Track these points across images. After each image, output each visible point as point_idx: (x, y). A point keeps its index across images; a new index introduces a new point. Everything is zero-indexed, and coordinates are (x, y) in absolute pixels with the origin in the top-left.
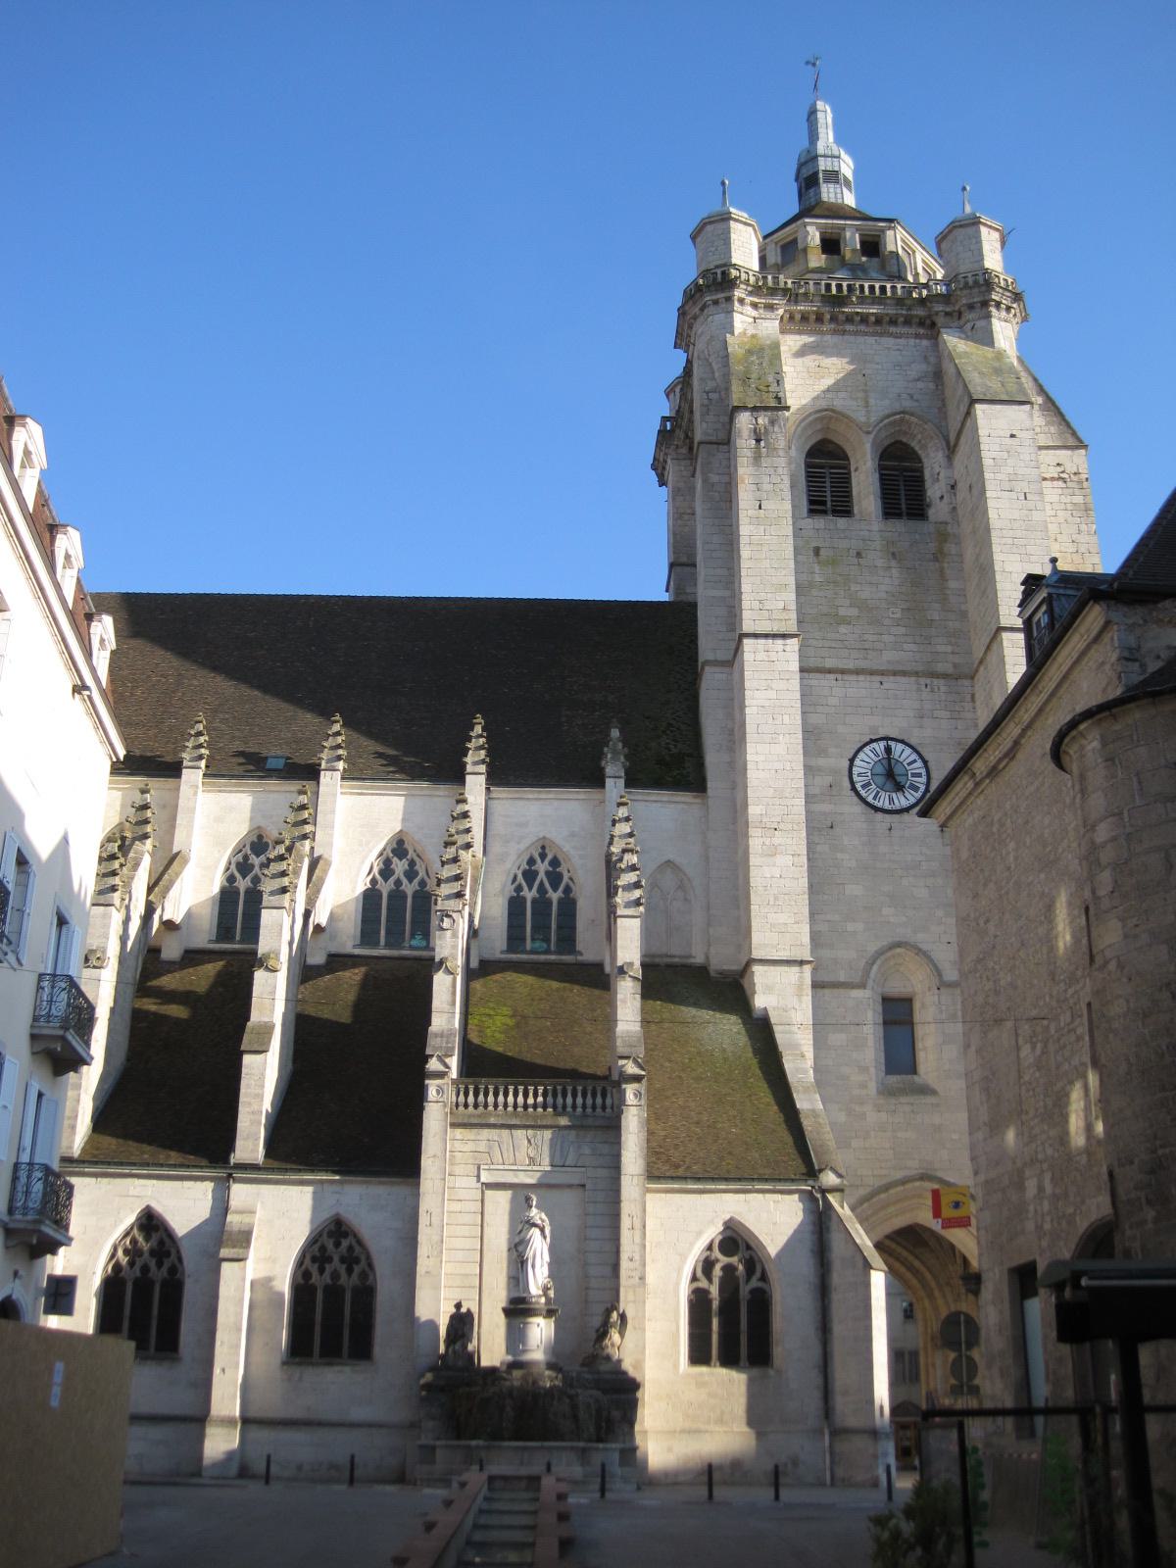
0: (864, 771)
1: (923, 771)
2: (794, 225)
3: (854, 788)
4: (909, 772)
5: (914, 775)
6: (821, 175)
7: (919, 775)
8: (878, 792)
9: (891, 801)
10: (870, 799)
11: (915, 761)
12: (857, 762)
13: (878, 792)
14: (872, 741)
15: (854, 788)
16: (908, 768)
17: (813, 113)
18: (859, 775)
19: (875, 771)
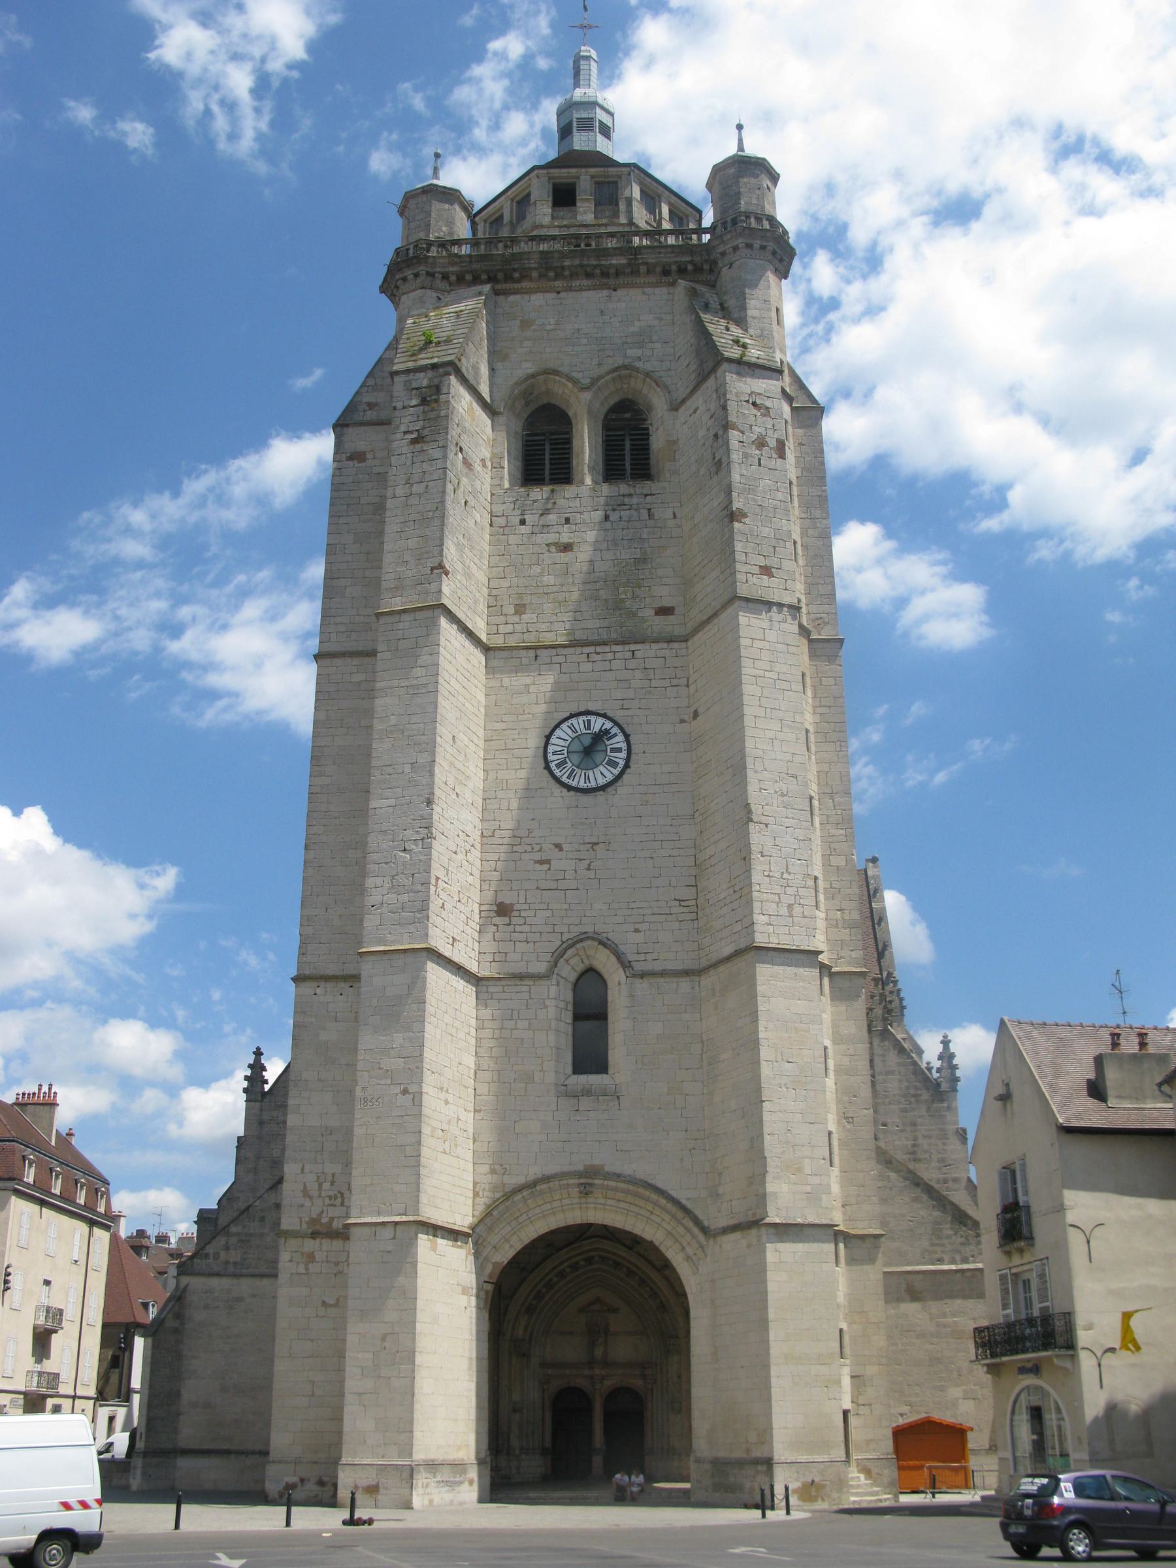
0: (563, 748)
1: (624, 746)
2: (527, 178)
3: (547, 767)
4: (608, 747)
5: (613, 750)
6: (575, 124)
7: (619, 750)
8: (573, 770)
9: (587, 779)
10: (564, 779)
12: (553, 740)
13: (573, 770)
15: (547, 767)
16: (607, 743)
19: (572, 749)
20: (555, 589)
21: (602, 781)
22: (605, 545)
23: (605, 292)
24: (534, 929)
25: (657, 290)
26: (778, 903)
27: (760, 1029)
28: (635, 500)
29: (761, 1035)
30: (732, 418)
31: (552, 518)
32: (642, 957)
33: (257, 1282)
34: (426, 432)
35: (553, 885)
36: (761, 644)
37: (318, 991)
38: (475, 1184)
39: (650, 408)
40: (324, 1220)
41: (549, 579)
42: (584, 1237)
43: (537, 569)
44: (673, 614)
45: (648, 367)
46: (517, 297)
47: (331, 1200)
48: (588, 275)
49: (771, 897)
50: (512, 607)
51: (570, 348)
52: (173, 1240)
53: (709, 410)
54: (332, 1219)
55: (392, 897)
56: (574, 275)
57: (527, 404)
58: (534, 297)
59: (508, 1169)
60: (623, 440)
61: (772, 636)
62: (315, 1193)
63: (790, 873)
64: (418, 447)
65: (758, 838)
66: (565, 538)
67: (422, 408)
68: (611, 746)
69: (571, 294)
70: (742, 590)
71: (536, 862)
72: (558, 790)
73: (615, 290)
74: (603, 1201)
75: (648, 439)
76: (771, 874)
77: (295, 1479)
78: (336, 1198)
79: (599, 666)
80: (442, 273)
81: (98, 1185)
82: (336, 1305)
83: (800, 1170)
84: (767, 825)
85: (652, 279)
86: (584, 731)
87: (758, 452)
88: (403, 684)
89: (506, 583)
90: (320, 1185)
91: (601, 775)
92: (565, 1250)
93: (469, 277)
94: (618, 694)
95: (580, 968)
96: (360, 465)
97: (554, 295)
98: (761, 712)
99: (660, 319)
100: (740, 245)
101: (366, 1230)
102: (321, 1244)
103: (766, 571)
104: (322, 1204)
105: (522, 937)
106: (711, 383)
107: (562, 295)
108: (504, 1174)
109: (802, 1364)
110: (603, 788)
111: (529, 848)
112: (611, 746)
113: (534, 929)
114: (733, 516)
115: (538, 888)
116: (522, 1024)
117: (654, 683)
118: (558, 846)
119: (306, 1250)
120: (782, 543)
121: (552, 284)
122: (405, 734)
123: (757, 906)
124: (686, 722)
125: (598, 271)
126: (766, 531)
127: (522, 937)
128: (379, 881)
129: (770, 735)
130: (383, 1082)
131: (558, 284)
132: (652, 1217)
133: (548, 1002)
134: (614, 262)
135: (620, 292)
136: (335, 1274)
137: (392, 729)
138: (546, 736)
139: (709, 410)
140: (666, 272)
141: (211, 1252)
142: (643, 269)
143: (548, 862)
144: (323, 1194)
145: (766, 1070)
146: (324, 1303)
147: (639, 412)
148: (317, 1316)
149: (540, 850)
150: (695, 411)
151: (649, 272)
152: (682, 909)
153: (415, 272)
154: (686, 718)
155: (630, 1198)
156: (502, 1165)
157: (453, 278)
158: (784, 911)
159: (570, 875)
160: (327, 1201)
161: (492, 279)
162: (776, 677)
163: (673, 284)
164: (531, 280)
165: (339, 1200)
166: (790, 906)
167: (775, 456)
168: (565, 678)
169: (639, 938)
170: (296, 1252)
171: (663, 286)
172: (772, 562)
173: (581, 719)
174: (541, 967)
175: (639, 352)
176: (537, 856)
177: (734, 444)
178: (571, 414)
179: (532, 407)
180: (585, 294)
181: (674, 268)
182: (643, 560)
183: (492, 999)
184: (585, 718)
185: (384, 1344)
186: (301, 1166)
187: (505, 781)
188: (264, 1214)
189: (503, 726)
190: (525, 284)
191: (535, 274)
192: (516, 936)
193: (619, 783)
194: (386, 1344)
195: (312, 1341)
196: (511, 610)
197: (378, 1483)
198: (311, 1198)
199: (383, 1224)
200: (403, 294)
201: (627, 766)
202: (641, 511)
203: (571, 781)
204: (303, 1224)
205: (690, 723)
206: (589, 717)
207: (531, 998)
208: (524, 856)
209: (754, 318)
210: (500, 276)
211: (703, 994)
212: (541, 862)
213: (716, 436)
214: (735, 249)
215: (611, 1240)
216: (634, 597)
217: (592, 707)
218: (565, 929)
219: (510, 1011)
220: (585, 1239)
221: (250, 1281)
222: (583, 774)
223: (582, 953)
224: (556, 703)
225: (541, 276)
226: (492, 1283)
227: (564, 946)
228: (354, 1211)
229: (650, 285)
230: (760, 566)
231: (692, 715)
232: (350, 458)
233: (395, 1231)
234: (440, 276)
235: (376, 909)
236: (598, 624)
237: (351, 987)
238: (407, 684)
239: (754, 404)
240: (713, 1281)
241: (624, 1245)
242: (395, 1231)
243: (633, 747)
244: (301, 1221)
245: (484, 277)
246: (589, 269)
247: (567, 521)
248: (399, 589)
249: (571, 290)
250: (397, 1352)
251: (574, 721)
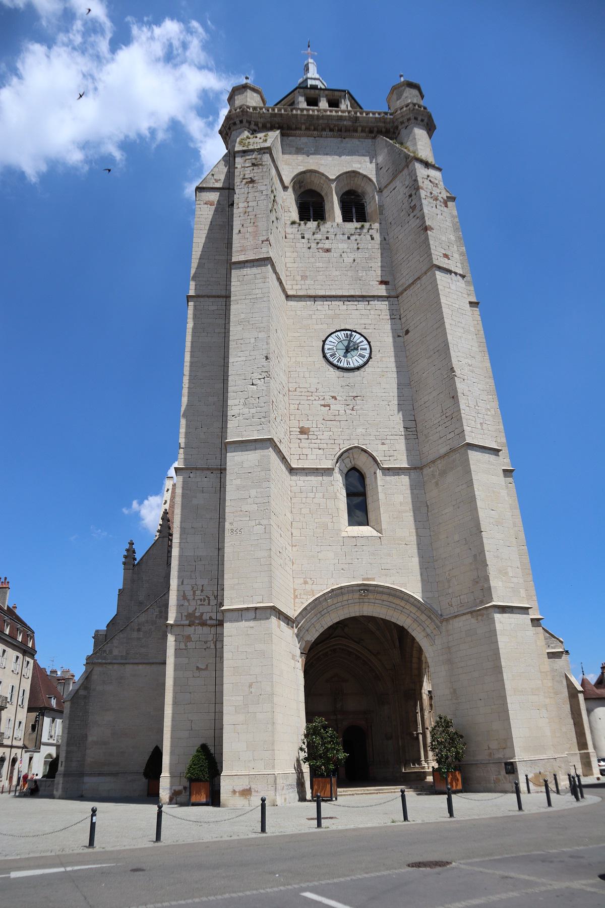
1: (367, 347)
2: (292, 94)
3: (325, 356)
4: (359, 348)
7: (365, 349)
9: (348, 363)
10: (335, 362)
11: (362, 341)
12: (327, 342)
14: (337, 331)
15: (325, 356)
17: (307, 64)
18: (328, 349)
20: (323, 269)
21: (357, 365)
22: (349, 250)
23: (339, 139)
24: (322, 442)
25: (366, 140)
26: (475, 422)
27: (475, 490)
29: (476, 493)
30: (420, 184)
31: (318, 236)
32: (387, 458)
33: (136, 667)
35: (333, 418)
36: (449, 290)
37: (191, 475)
38: (295, 590)
39: (364, 193)
40: (197, 614)
41: (321, 265)
42: (332, 636)
43: (312, 260)
44: (388, 285)
46: (294, 138)
47: (201, 601)
48: (331, 130)
49: (471, 418)
50: (300, 277)
51: (323, 161)
52: (59, 673)
53: (405, 184)
54: (202, 614)
55: (246, 410)
56: (323, 129)
57: (300, 187)
58: (302, 138)
59: (315, 581)
60: (352, 208)
61: (453, 287)
62: (191, 597)
63: (478, 406)
64: (251, 185)
65: (460, 386)
66: (327, 246)
67: (252, 168)
68: (361, 347)
69: (321, 139)
70: (435, 262)
71: (322, 405)
72: (331, 369)
73: (344, 138)
74: (373, 601)
75: (364, 208)
76: (469, 405)
77: (181, 788)
78: (204, 600)
79: (350, 307)
80: (255, 122)
81: (29, 633)
82: (206, 669)
83: (506, 573)
84: (464, 380)
85: (364, 134)
86: (345, 339)
87: (434, 202)
88: (247, 298)
89: (296, 265)
90: (194, 592)
91: (355, 360)
92: (321, 645)
93: (269, 125)
94: (363, 322)
95: (349, 466)
96: (211, 207)
97: (313, 138)
98: (453, 323)
99: (369, 153)
100: (411, 118)
101: (236, 613)
102: (195, 630)
103: (446, 256)
104: (195, 604)
105: (316, 446)
106: (405, 172)
107: (316, 138)
108: (313, 584)
109: (523, 695)
110: (358, 368)
111: (317, 398)
112: (361, 347)
113: (322, 442)
114: (427, 229)
115: (323, 419)
116: (320, 495)
117: (381, 317)
118: (334, 398)
119: (186, 633)
120: (452, 245)
121: (311, 132)
122: (250, 323)
123: (464, 421)
124: (401, 336)
125: (337, 128)
126: (443, 238)
127: (316, 446)
128: (236, 402)
129: (460, 335)
130: (245, 519)
131: (315, 133)
132: (403, 610)
133: (333, 483)
134: (345, 123)
135: (347, 139)
136: (205, 649)
137: (242, 320)
138: (323, 341)
139: (405, 184)
140: (371, 132)
141: (108, 650)
142: (360, 129)
143: (329, 406)
144: (196, 598)
145: (482, 514)
146: (198, 668)
147: (358, 196)
148: (193, 677)
149: (323, 399)
150: (394, 189)
151: (362, 131)
152: (409, 433)
153: (240, 119)
154: (401, 335)
155: (391, 599)
156: (311, 579)
157: (260, 125)
158: (479, 426)
159: (342, 412)
160: (199, 602)
161: (280, 127)
162: (458, 307)
163: (374, 138)
164: (301, 130)
165: (207, 601)
166: (481, 424)
167: (443, 206)
168: (331, 312)
169: (385, 447)
170: (178, 635)
171: (369, 139)
172: (448, 253)
173: (342, 332)
174: (328, 464)
175: (359, 166)
176: (323, 402)
177: (423, 196)
178: (323, 194)
179: (302, 190)
180: (328, 139)
181: (376, 129)
183: (300, 480)
184: (344, 332)
185: (251, 690)
186: (182, 580)
187: (301, 363)
188: (140, 627)
189: (297, 334)
190: (298, 132)
191: (303, 127)
192: (312, 446)
193: (367, 366)
194: (253, 690)
195: (190, 693)
196: (299, 278)
197: (250, 788)
198: (188, 600)
199: (247, 609)
200: (234, 130)
201: (370, 357)
202: (367, 236)
203: (339, 364)
204: (183, 616)
205: (403, 337)
206: (347, 332)
207: (323, 480)
208: (314, 402)
209: (421, 150)
210: (285, 126)
211: (425, 479)
212: (324, 406)
213: (410, 196)
214: (409, 120)
215: (348, 639)
217: (348, 328)
218: (341, 442)
219: (311, 488)
220: (332, 638)
221: (131, 666)
222: (346, 360)
223: (351, 456)
224: (328, 324)
225: (307, 129)
226: (304, 654)
227: (342, 451)
228: (226, 602)
229: (362, 137)
230: (443, 254)
231: (404, 333)
232: (206, 204)
233: (256, 614)
234: (254, 123)
235: (236, 417)
236: (348, 287)
237: (212, 473)
238: (251, 297)
239: (430, 181)
240: (449, 648)
241: (355, 641)
242: (256, 614)
243: (372, 348)
244: (182, 615)
245: (277, 126)
246: (332, 126)
248: (243, 250)
249: (322, 137)
250: (261, 695)
251: (338, 333)
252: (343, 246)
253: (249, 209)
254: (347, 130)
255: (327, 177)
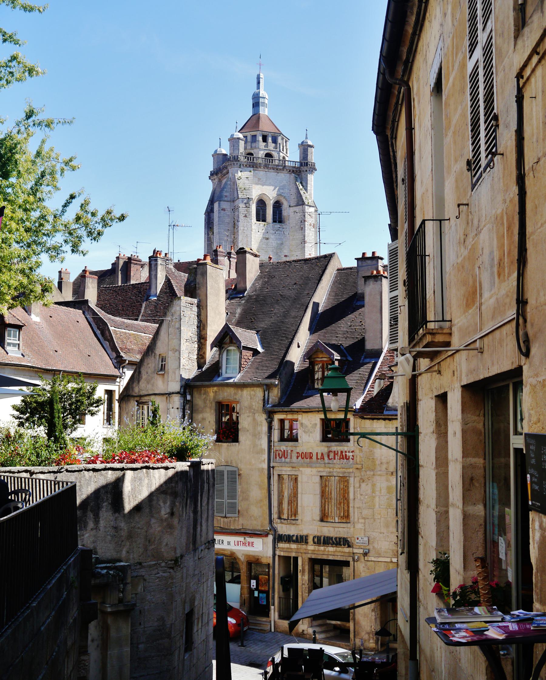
23: (276, 173)
28: (281, 229)
30: (306, 219)
34: (247, 215)
39: (283, 204)
45: (284, 195)
48: (273, 169)
85: (286, 172)
131: (267, 170)
135: (279, 174)
147: (280, 204)
157: (244, 166)
172: (311, 253)
177: (306, 225)
182: (282, 244)
190: (260, 169)
216: (280, 252)
232: (222, 210)
247: (267, 232)
252: (272, 237)
253: (245, 231)
254: (280, 169)
255: (269, 198)
